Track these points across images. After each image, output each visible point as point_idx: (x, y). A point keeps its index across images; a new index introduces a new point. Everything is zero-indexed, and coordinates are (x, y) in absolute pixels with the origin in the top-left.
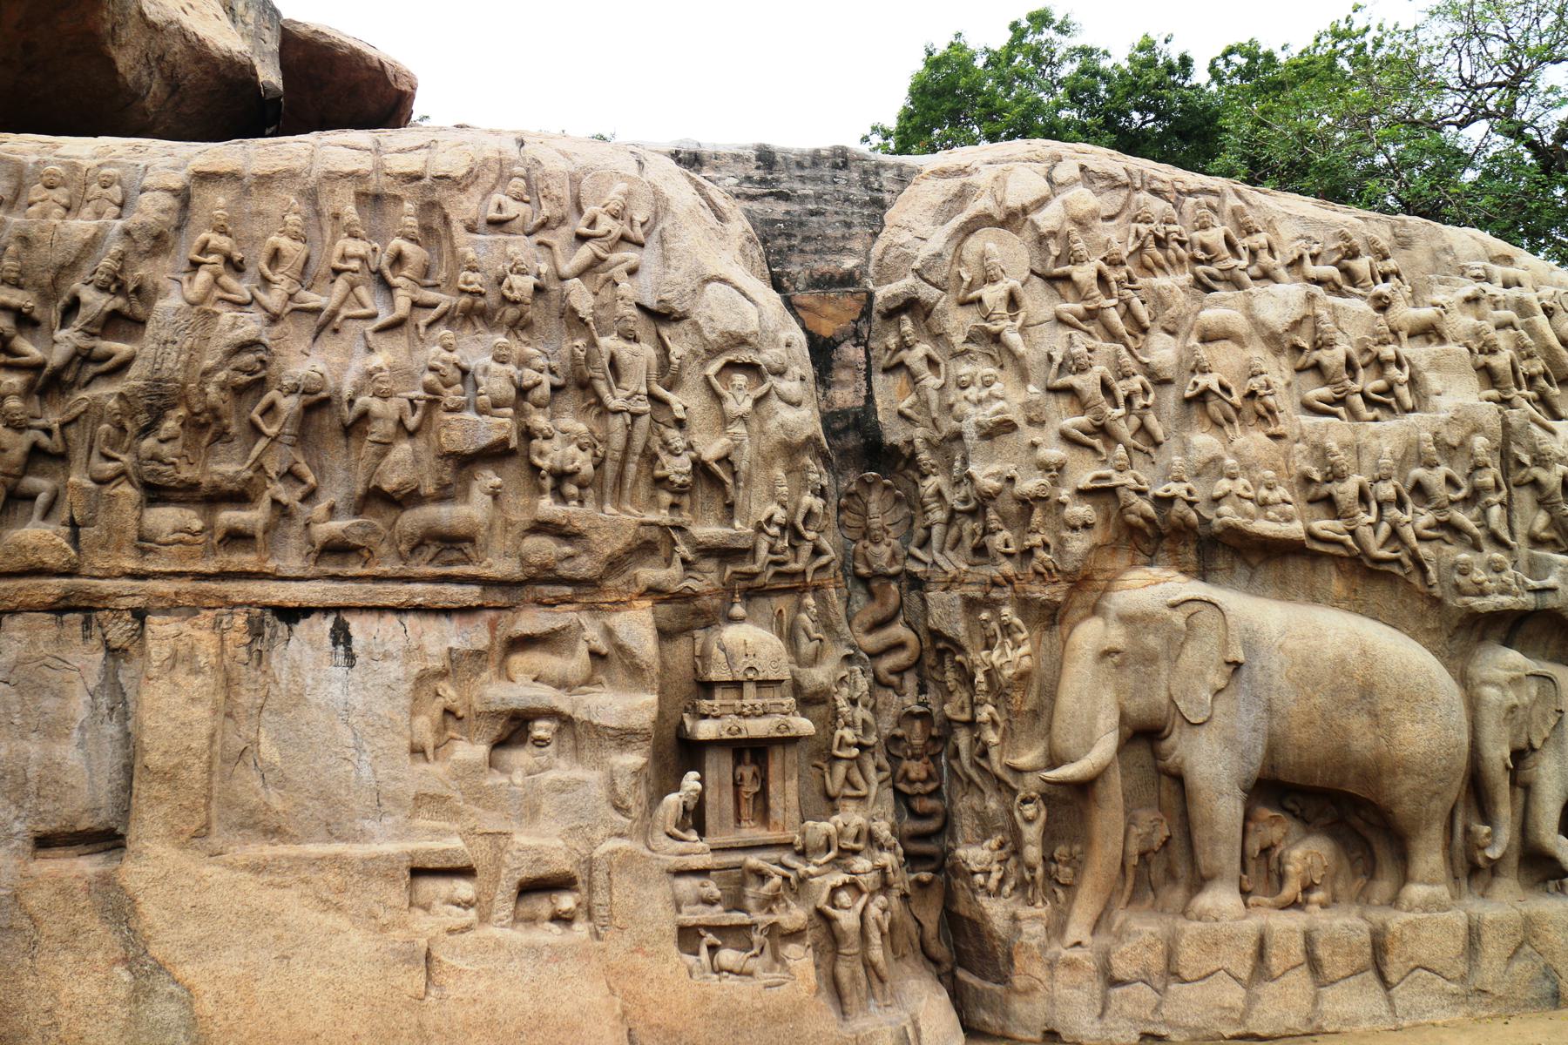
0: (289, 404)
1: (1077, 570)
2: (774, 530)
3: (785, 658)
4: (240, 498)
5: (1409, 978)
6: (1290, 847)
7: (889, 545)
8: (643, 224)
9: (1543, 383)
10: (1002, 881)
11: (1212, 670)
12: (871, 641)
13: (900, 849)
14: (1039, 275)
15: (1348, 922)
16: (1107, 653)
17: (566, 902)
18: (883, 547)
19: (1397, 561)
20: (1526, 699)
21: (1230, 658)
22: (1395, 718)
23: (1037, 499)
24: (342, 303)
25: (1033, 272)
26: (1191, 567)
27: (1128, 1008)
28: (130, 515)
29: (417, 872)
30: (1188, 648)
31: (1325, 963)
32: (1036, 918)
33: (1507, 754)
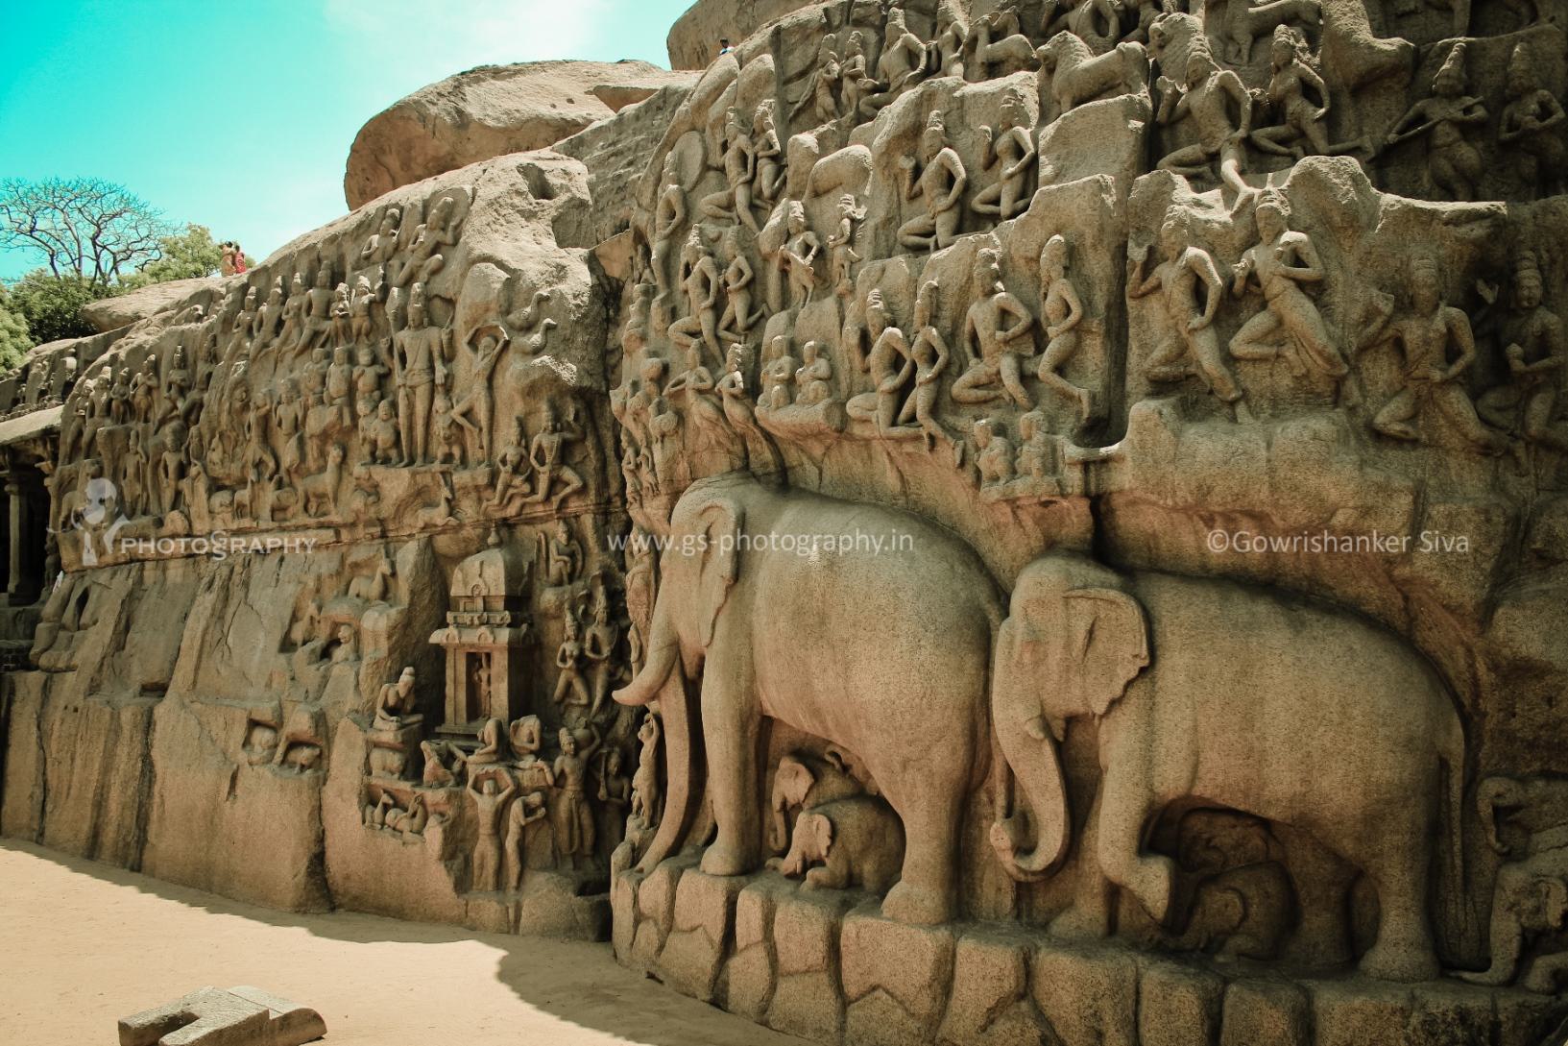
0: (251, 417)
2: (509, 468)
3: (502, 579)
4: (242, 482)
8: (456, 228)
9: (1296, 105)
13: (614, 760)
14: (716, 169)
17: (304, 755)
24: (284, 343)
25: (706, 167)
28: (205, 496)
29: (254, 724)
30: (709, 567)
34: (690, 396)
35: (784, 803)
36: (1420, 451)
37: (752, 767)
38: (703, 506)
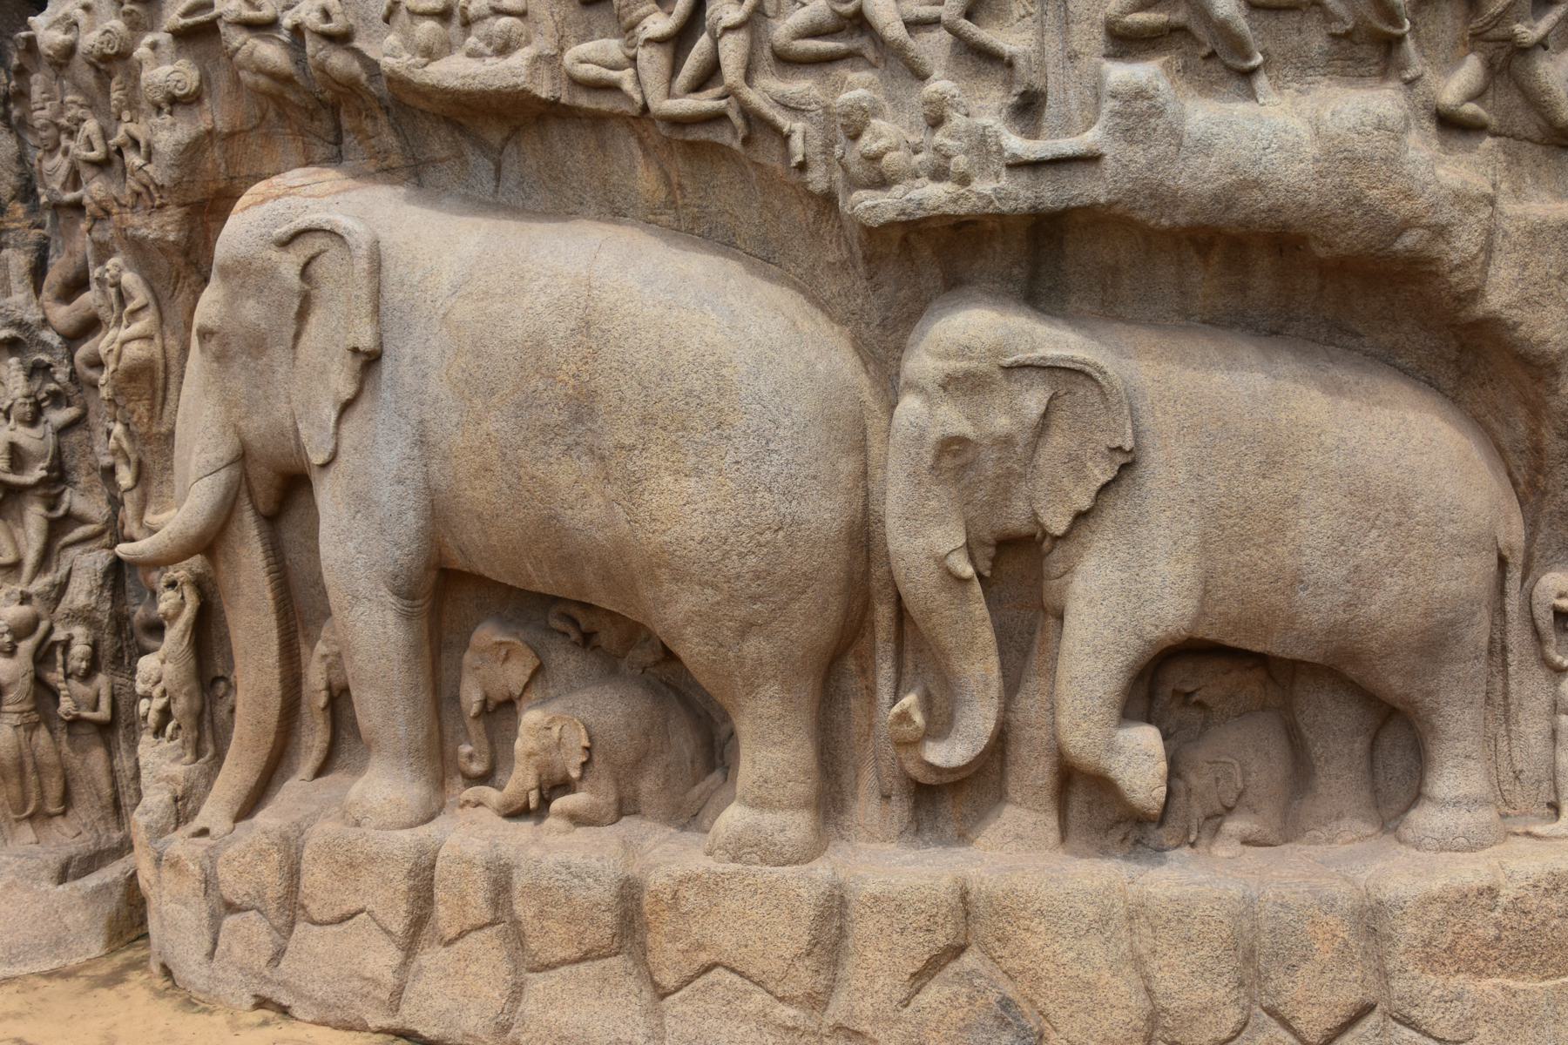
1: (178, 183)
5: (699, 983)
6: (544, 701)
7: (66, 152)
10: (166, 713)
11: (336, 367)
12: (63, 315)
13: (79, 649)
15: (576, 859)
16: (205, 334)
18: (59, 156)
19: (718, 118)
20: (1002, 423)
21: (351, 343)
22: (638, 463)
23: (105, 58)
26: (395, 160)
27: (238, 950)
31: (527, 929)
32: (171, 779)
33: (948, 539)
34: (236, 39)
35: (485, 702)
36: (1488, 142)
37: (427, 650)
38: (285, 229)
